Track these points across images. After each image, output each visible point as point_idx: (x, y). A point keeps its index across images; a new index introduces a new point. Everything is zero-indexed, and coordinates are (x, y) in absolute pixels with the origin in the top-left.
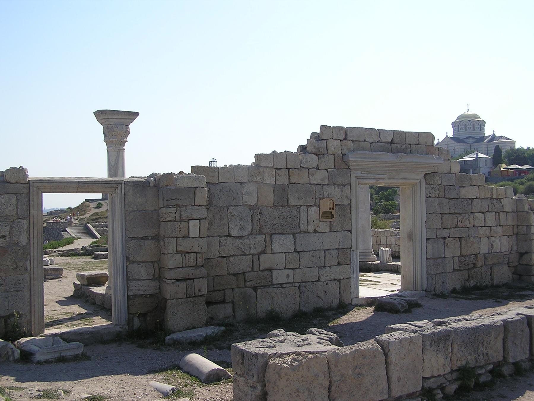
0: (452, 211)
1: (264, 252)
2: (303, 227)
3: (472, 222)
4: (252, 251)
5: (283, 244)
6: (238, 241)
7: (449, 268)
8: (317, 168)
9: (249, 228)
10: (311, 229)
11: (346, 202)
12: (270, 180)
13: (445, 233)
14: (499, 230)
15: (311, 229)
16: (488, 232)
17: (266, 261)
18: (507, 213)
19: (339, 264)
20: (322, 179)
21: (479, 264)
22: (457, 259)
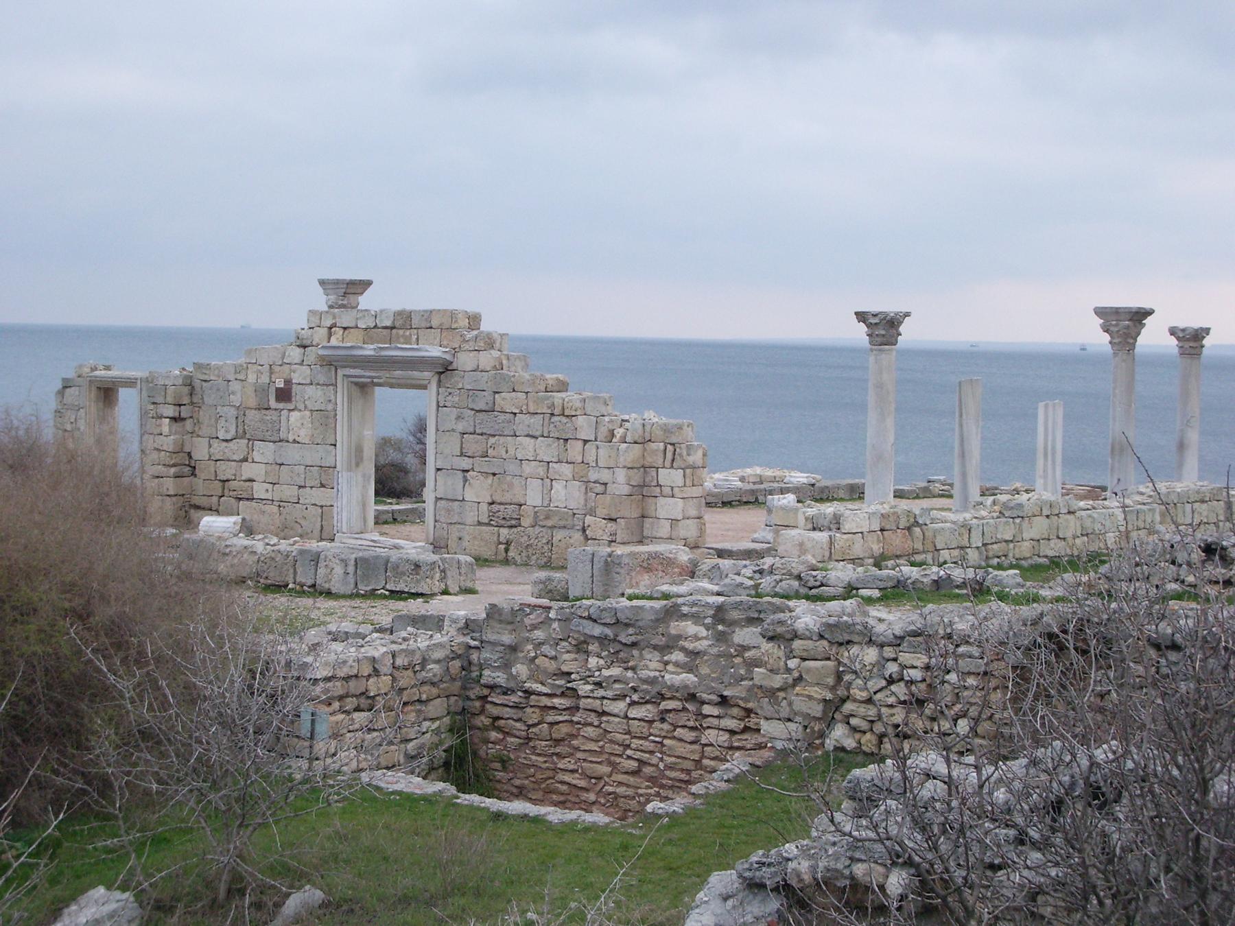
0: (478, 431)
1: (245, 460)
2: (283, 435)
3: (512, 452)
4: (235, 457)
5: (264, 452)
6: (225, 444)
7: (471, 517)
8: (302, 364)
9: (233, 432)
10: (291, 439)
11: (330, 407)
12: (252, 378)
13: (465, 463)
14: (566, 470)
15: (291, 439)
16: (541, 471)
17: (248, 470)
18: (586, 442)
19: (323, 486)
20: (305, 378)
21: (526, 522)
22: (484, 507)
